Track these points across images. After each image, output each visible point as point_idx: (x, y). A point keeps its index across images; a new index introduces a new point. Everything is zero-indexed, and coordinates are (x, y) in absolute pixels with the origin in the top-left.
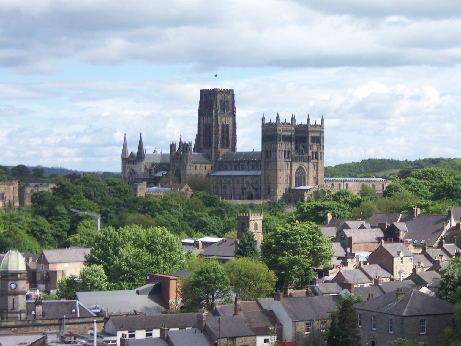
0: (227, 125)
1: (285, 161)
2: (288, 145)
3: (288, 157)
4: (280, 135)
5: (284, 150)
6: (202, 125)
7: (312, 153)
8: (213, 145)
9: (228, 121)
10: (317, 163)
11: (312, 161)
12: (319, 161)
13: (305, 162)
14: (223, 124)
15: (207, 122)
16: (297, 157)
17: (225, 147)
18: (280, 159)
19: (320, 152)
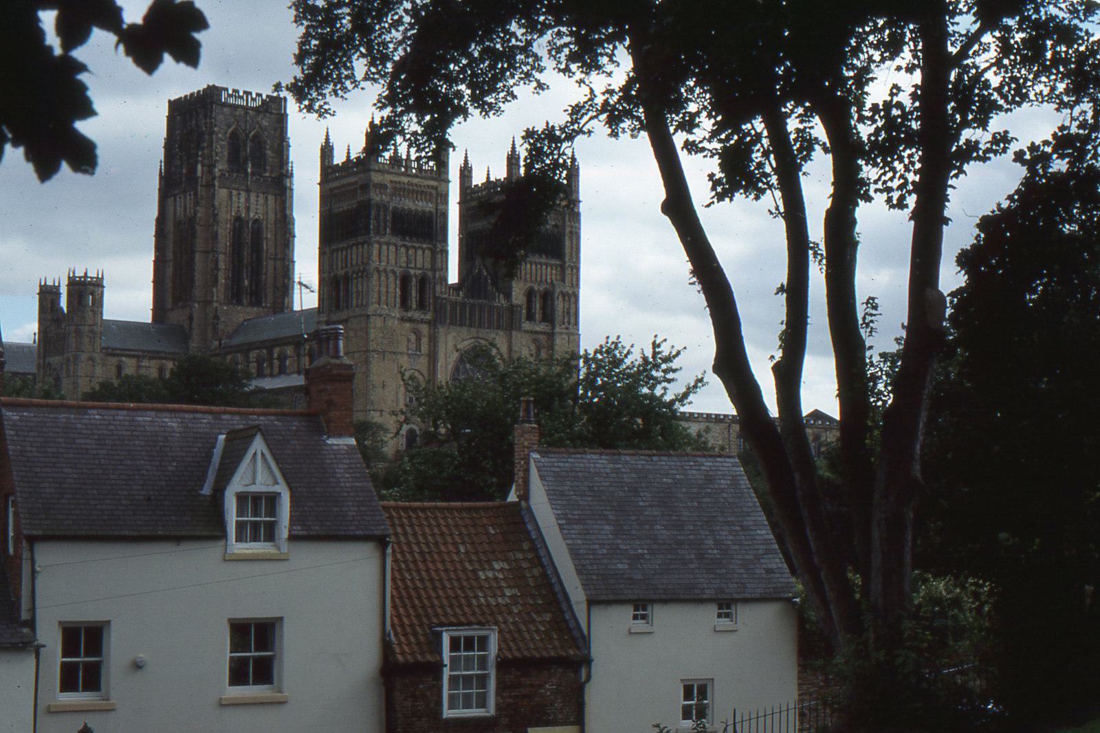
0: (256, 221)
1: (402, 319)
2: (420, 252)
3: (422, 306)
4: (382, 207)
5: (398, 271)
6: (170, 226)
7: (530, 294)
8: (198, 292)
9: (258, 207)
10: (551, 336)
11: (527, 326)
12: (557, 329)
13: (498, 328)
14: (238, 218)
15: (185, 211)
16: (463, 305)
17: (245, 302)
18: (384, 309)
19: (564, 295)
